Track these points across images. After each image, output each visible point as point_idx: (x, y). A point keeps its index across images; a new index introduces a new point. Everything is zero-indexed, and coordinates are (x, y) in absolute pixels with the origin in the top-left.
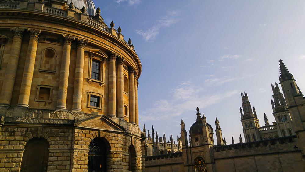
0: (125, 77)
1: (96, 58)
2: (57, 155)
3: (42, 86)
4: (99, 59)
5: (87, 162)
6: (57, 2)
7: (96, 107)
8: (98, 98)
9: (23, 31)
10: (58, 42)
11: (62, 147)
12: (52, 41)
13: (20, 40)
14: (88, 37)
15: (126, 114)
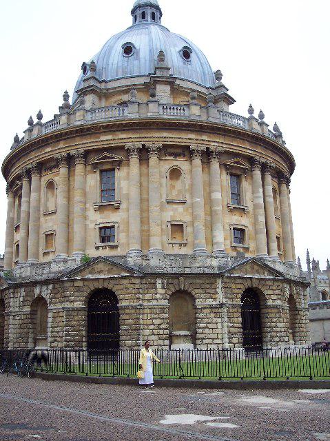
0: (274, 190)
1: (234, 171)
2: (205, 311)
3: (173, 223)
4: (238, 173)
5: (240, 319)
6: (163, 81)
7: (241, 245)
8: (242, 231)
9: (140, 146)
10: (184, 156)
11: (210, 302)
12: (176, 155)
13: (138, 160)
14: (223, 143)
15: (279, 249)
